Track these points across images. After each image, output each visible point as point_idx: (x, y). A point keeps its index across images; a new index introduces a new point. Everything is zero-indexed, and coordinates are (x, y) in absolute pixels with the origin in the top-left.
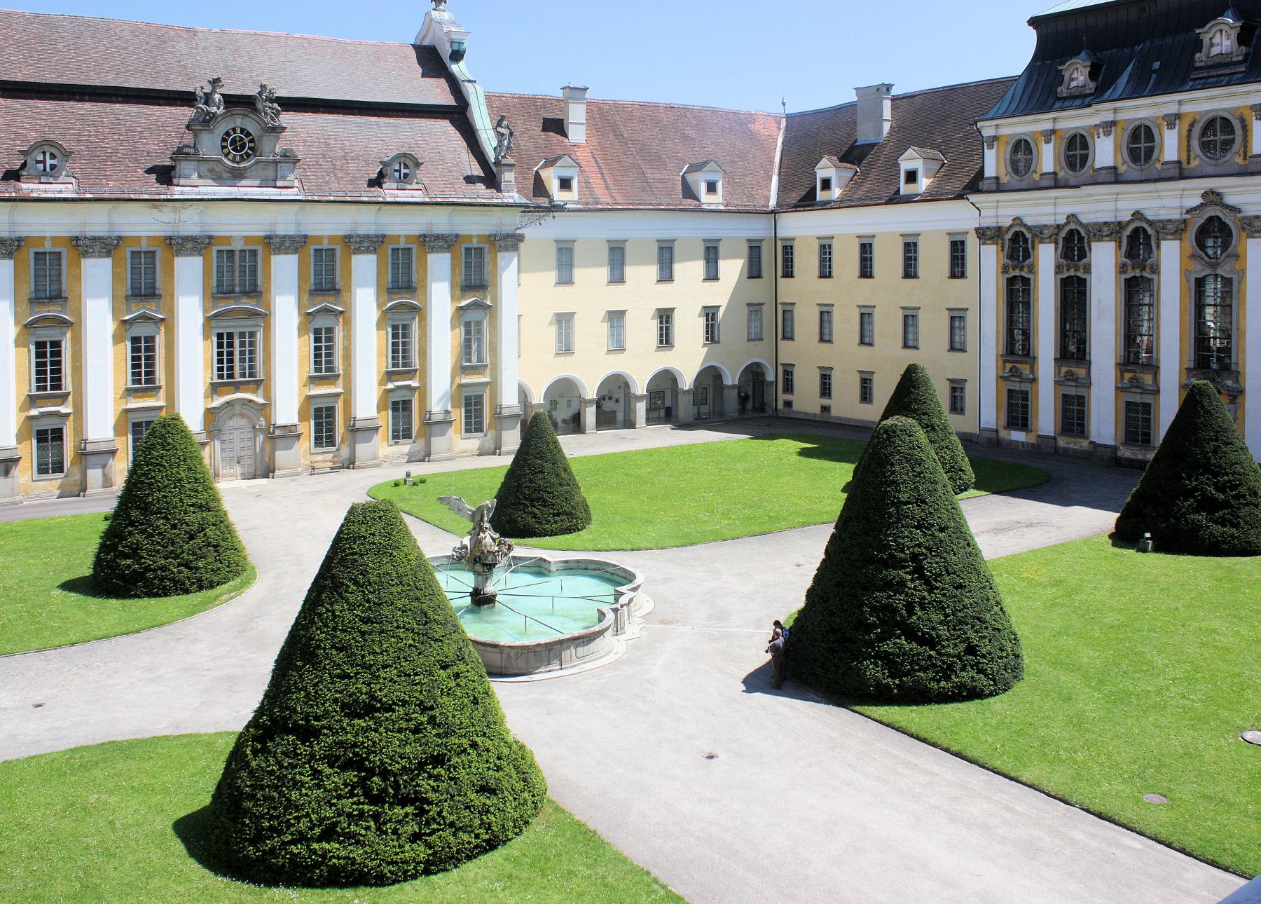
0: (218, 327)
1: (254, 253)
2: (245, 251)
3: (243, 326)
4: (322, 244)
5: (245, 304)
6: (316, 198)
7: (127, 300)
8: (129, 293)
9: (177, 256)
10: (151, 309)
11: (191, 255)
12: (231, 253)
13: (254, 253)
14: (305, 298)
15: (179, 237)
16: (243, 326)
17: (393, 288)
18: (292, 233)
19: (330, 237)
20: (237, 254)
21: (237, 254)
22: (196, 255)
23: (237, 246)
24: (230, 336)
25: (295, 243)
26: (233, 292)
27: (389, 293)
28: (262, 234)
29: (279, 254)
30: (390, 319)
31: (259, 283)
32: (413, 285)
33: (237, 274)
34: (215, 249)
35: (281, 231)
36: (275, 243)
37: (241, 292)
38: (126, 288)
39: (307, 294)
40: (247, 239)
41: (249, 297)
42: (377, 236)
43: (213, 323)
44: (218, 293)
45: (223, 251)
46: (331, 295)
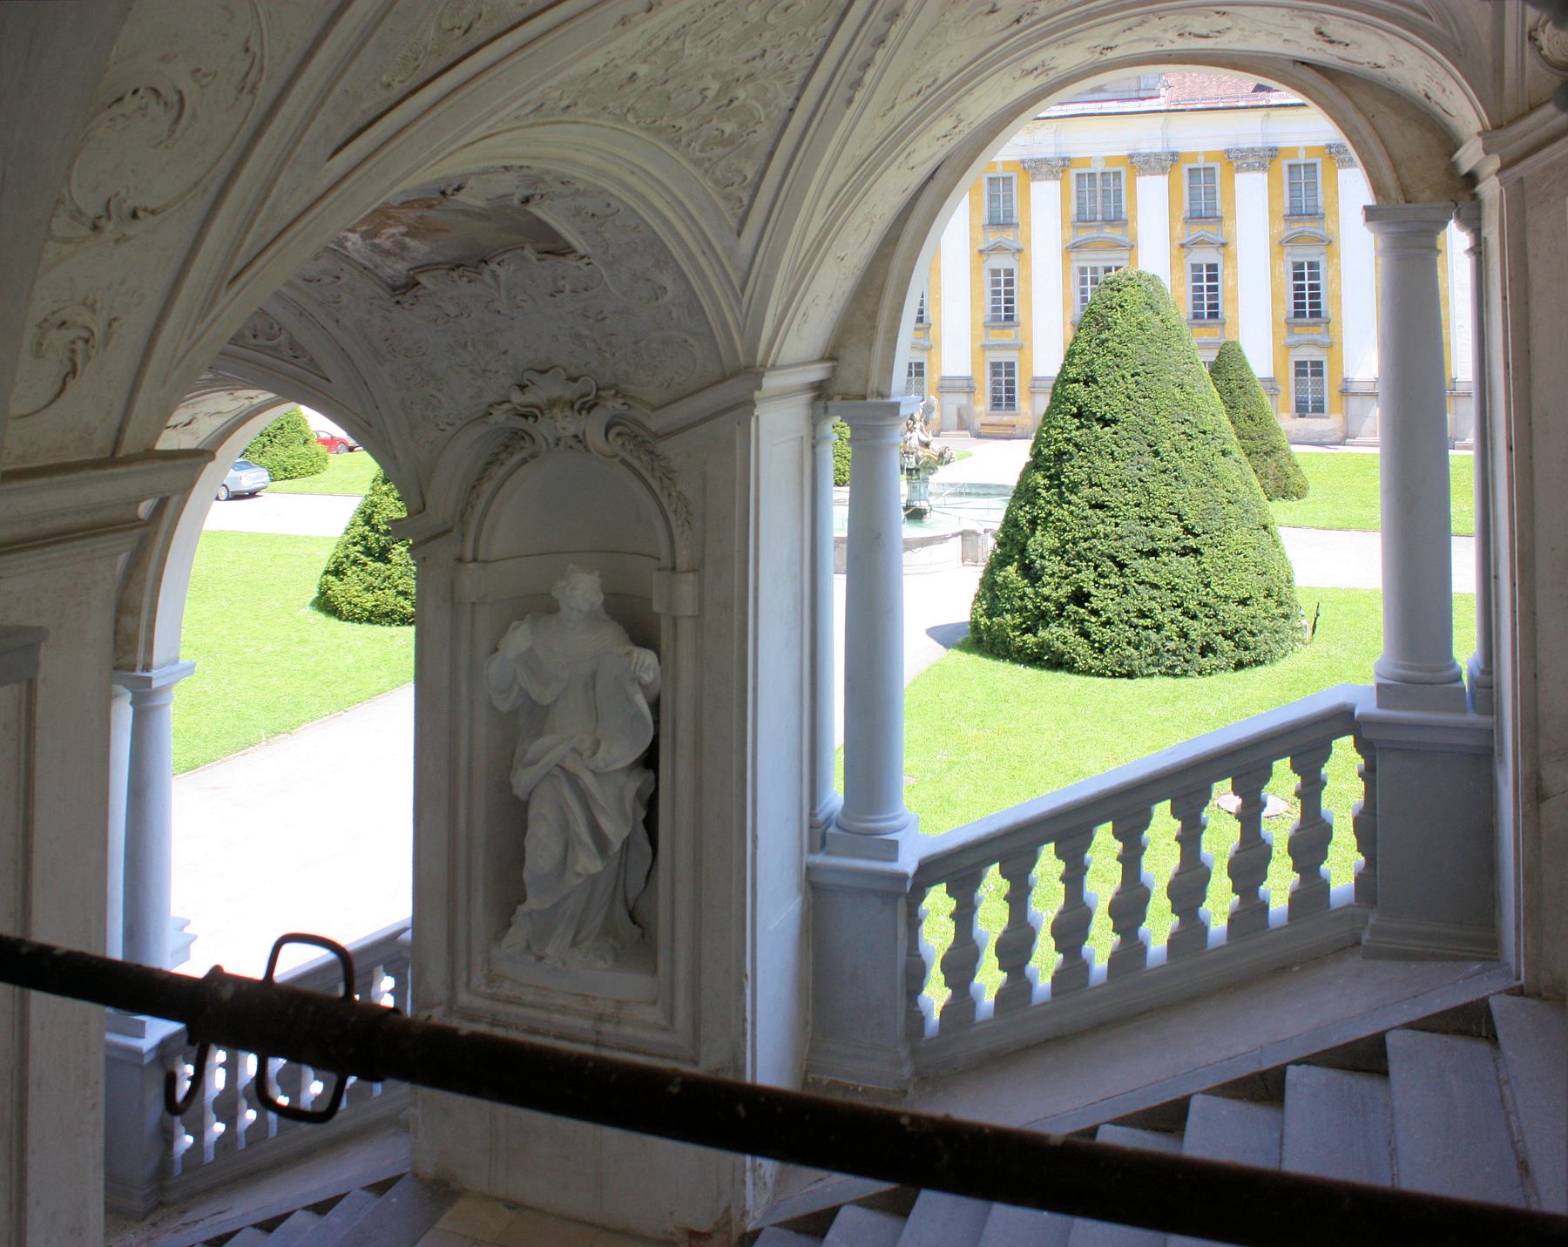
0: (1078, 260)
1: (1117, 175)
2: (1108, 173)
3: (1106, 260)
4: (1197, 162)
5: (1107, 233)
6: (1180, 107)
7: (984, 229)
8: (987, 222)
9: (1033, 180)
10: (1008, 237)
11: (1047, 179)
12: (1094, 174)
13: (1117, 175)
14: (1179, 227)
15: (1030, 160)
16: (1106, 260)
17: (1291, 215)
18: (1159, 150)
19: (1206, 154)
20: (1098, 177)
21: (1098, 177)
22: (1051, 179)
23: (1098, 168)
24: (1094, 270)
25: (1167, 162)
26: (1095, 220)
27: (1286, 220)
28: (1125, 153)
29: (1143, 175)
30: (1290, 254)
31: (1124, 210)
32: (1320, 210)
33: (1099, 199)
34: (1073, 172)
35: (1145, 148)
36: (1141, 163)
37: (1103, 220)
38: (984, 217)
39: (1182, 222)
40: (1109, 160)
41: (1113, 226)
42: (1263, 149)
43: (1074, 256)
44: (1078, 221)
45: (1084, 174)
46: (1210, 223)
